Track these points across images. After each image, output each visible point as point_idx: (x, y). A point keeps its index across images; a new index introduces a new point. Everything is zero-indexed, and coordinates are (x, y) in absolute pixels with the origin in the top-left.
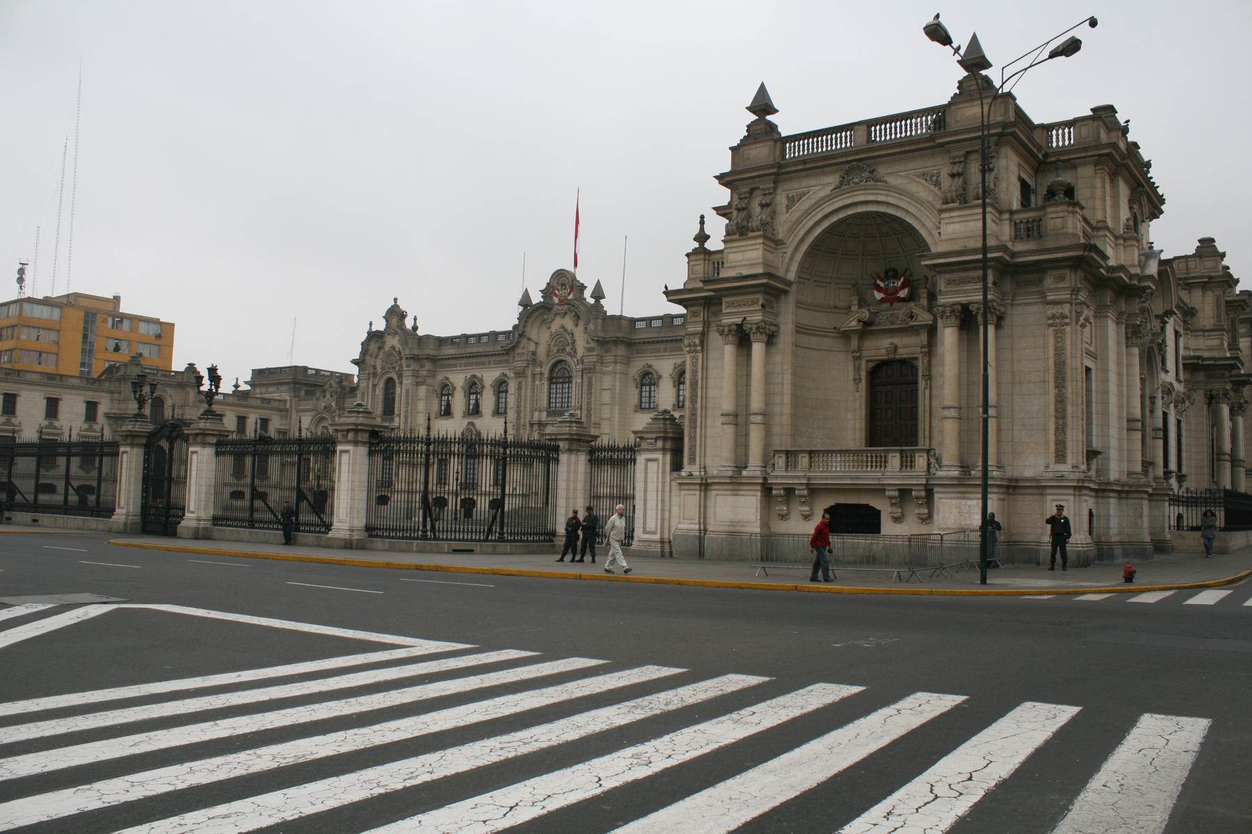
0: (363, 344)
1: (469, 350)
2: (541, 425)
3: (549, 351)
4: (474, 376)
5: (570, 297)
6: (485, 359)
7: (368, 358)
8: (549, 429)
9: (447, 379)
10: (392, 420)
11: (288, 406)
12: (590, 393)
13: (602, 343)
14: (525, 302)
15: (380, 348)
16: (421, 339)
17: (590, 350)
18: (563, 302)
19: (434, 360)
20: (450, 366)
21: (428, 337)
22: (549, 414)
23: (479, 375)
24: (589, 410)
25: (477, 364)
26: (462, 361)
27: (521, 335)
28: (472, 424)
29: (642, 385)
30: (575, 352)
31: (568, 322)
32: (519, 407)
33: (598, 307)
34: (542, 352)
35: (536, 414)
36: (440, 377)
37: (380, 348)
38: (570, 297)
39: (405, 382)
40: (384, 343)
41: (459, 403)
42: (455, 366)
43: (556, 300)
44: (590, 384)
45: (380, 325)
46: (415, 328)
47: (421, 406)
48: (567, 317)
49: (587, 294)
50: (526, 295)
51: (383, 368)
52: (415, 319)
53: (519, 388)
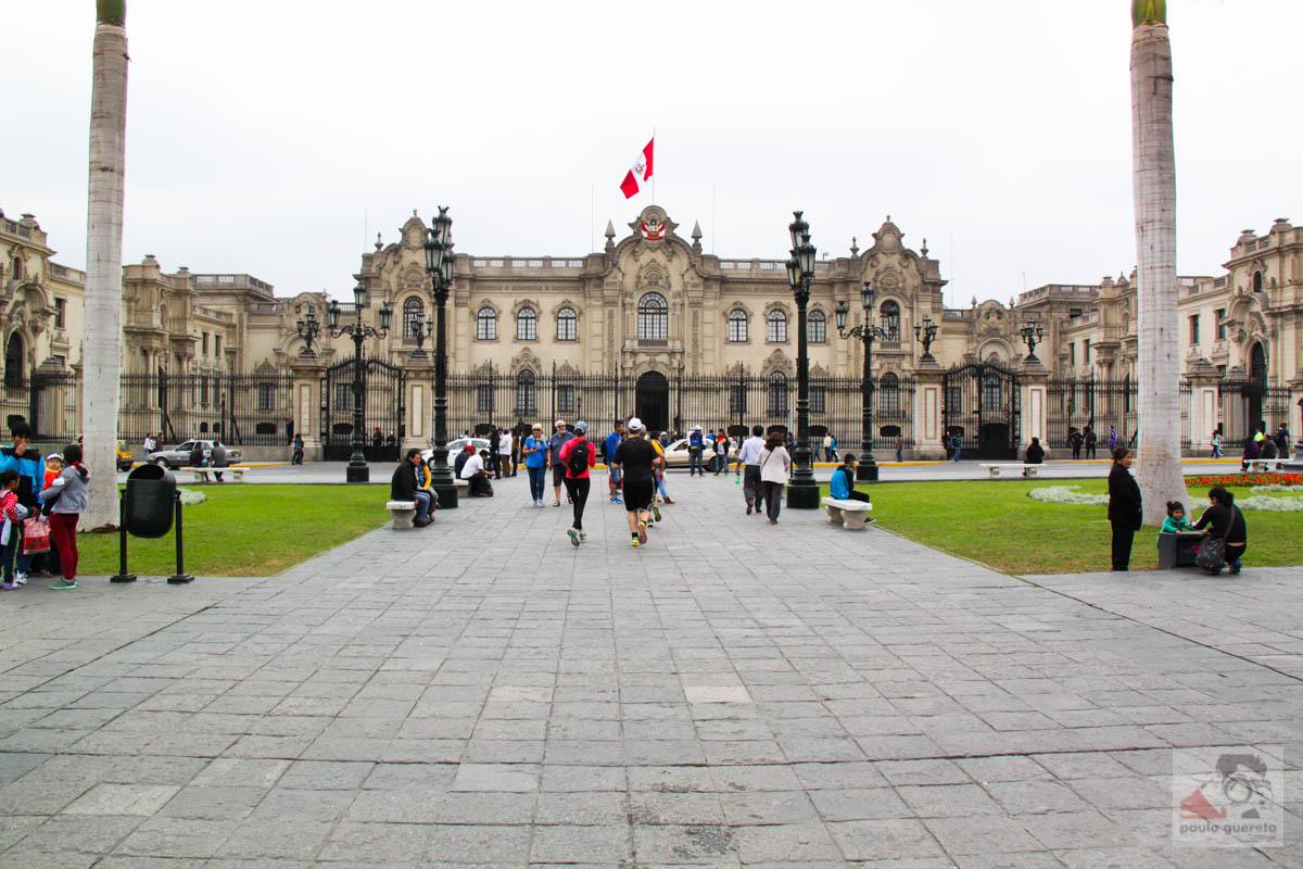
0: (367, 258)
2: (634, 353)
5: (662, 234)
6: (543, 285)
7: (383, 272)
8: (642, 358)
11: (235, 321)
12: (695, 325)
15: (395, 263)
17: (695, 285)
19: (474, 280)
20: (490, 288)
22: (641, 343)
24: (695, 342)
25: (529, 288)
26: (510, 284)
27: (614, 265)
30: (670, 286)
31: (660, 257)
32: (611, 334)
33: (697, 246)
34: (629, 282)
35: (628, 343)
36: (478, 300)
37: (395, 263)
38: (662, 234)
40: (401, 257)
41: (506, 326)
42: (500, 288)
43: (645, 234)
47: (462, 329)
48: (659, 253)
50: (610, 224)
51: (400, 288)
53: (611, 316)
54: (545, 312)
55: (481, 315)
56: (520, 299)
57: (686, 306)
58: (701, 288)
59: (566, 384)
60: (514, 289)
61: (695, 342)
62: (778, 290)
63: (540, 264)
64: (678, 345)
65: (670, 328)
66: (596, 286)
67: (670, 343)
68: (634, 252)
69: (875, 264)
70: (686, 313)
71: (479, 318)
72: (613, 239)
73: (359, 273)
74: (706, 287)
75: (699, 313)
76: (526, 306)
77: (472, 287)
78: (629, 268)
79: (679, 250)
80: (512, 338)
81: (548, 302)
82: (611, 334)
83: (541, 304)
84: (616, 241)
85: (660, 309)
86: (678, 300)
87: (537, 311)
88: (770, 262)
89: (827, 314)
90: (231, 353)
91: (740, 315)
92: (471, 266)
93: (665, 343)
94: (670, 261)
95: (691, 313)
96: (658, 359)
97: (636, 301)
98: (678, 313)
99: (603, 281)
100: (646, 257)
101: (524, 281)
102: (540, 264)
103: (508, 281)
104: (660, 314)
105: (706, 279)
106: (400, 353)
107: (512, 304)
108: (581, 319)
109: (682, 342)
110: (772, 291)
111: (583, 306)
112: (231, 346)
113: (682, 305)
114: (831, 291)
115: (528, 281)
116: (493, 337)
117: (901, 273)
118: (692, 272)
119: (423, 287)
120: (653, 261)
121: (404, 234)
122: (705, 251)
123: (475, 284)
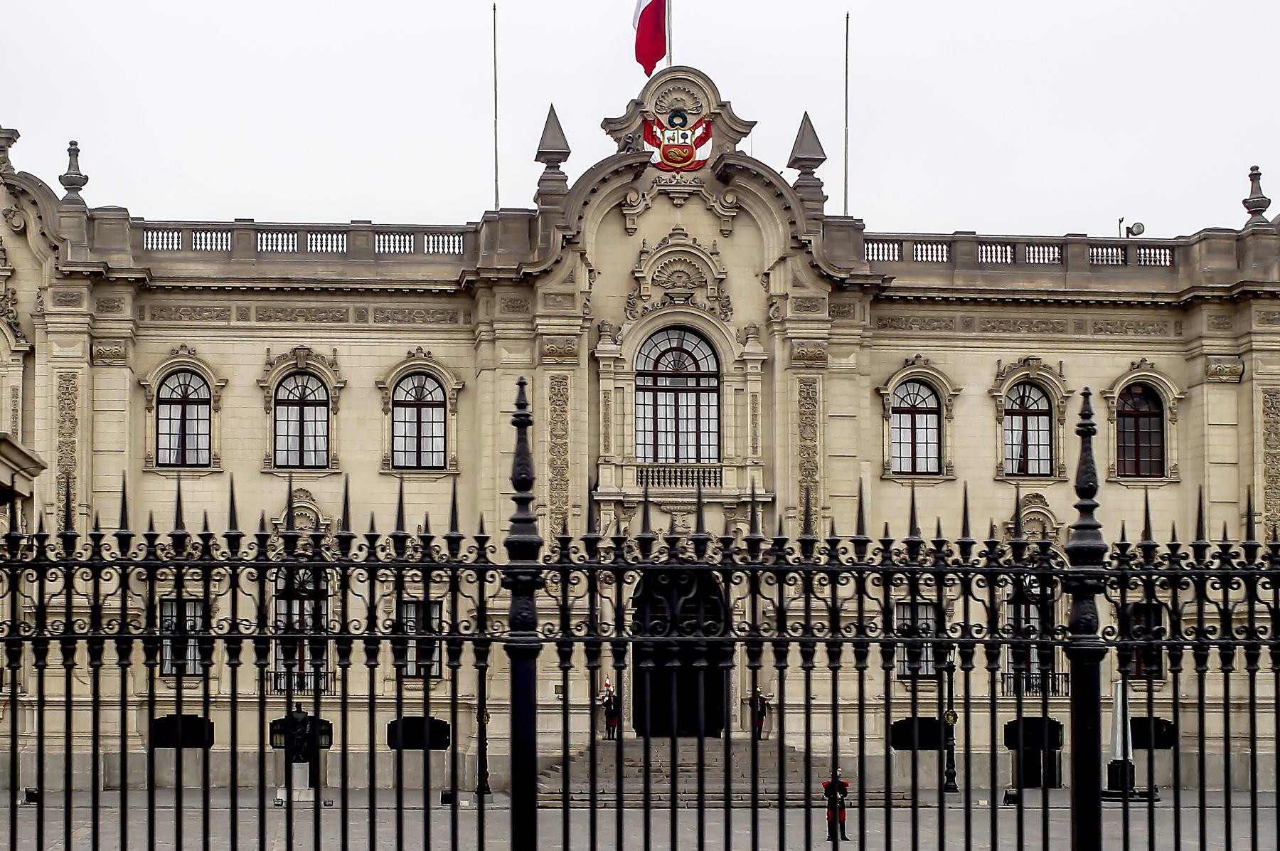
4: (302, 353)
9: (192, 353)
13: (839, 287)
14: (552, 153)
17: (806, 304)
18: (678, 160)
20: (195, 313)
21: (120, 214)
22: (644, 476)
23: (321, 347)
24: (808, 470)
25: (308, 315)
26: (253, 303)
31: (697, 223)
34: (608, 295)
36: (157, 348)
41: (241, 426)
42: (223, 314)
44: (808, 398)
48: (695, 208)
52: (74, 151)
54: (353, 382)
55: (165, 393)
56: (282, 347)
57: (779, 366)
58: (825, 315)
60: (264, 316)
61: (808, 470)
62: (1030, 326)
63: (338, 244)
65: (728, 432)
66: (514, 307)
67: (729, 477)
68: (620, 205)
70: (778, 386)
71: (160, 401)
72: (563, 167)
74: (837, 312)
75: (819, 386)
76: (301, 366)
77: (139, 311)
78: (610, 257)
80: (258, 464)
81: (364, 356)
83: (343, 361)
84: (573, 170)
85: (698, 376)
86: (753, 348)
87: (332, 382)
88: (1003, 242)
89: (1171, 393)
91: (926, 396)
92: (141, 253)
95: (797, 386)
97: (629, 350)
98: (754, 386)
99: (532, 288)
100: (656, 223)
101: (295, 291)
102: (338, 244)
103: (250, 290)
104: (698, 391)
105: (839, 287)
107: (261, 361)
108: (463, 405)
109: (769, 472)
110: (1014, 326)
111: (466, 367)
113: (767, 364)
114: (1178, 325)
115: (310, 291)
116: (204, 458)
118: (797, 263)
120: (677, 232)
122: (832, 208)
123: (149, 301)
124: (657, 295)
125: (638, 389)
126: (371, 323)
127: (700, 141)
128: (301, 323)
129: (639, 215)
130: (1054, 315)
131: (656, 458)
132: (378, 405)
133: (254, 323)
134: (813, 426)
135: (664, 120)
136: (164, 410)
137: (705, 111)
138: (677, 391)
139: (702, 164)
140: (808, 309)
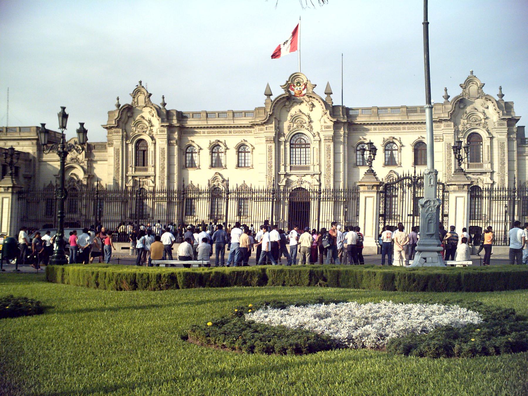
1: (211, 123)
2: (286, 175)
3: (289, 127)
10: (146, 170)
16: (168, 112)
17: (328, 127)
23: (222, 140)
25: (218, 132)
26: (206, 130)
28: (220, 174)
29: (357, 150)
30: (312, 128)
32: (270, 163)
35: (282, 168)
37: (129, 117)
39: (158, 142)
40: (132, 113)
41: (203, 158)
45: (129, 101)
46: (164, 104)
49: (320, 91)
53: (270, 150)
55: (188, 151)
56: (213, 140)
58: (332, 129)
59: (243, 197)
60: (208, 133)
64: (317, 170)
67: (312, 167)
69: (462, 106)
73: (105, 123)
79: (316, 103)
81: (232, 140)
82: (270, 163)
85: (306, 144)
86: (317, 138)
90: (28, 178)
93: (308, 168)
94: (312, 110)
96: (304, 179)
104: (306, 148)
106: (133, 177)
112: (27, 173)
113: (320, 141)
117: (484, 113)
119: (148, 133)
121: (134, 98)
124: (295, 125)
125: (291, 148)
126: (233, 134)
127: (304, 89)
128: (217, 134)
129: (290, 108)
130: (397, 126)
131: (296, 164)
132: (235, 152)
133: (206, 135)
134: (330, 155)
135: (295, 84)
136: (188, 155)
137: (304, 82)
138: (301, 148)
139: (304, 95)
140: (327, 128)
